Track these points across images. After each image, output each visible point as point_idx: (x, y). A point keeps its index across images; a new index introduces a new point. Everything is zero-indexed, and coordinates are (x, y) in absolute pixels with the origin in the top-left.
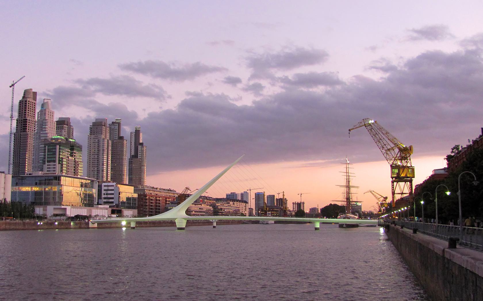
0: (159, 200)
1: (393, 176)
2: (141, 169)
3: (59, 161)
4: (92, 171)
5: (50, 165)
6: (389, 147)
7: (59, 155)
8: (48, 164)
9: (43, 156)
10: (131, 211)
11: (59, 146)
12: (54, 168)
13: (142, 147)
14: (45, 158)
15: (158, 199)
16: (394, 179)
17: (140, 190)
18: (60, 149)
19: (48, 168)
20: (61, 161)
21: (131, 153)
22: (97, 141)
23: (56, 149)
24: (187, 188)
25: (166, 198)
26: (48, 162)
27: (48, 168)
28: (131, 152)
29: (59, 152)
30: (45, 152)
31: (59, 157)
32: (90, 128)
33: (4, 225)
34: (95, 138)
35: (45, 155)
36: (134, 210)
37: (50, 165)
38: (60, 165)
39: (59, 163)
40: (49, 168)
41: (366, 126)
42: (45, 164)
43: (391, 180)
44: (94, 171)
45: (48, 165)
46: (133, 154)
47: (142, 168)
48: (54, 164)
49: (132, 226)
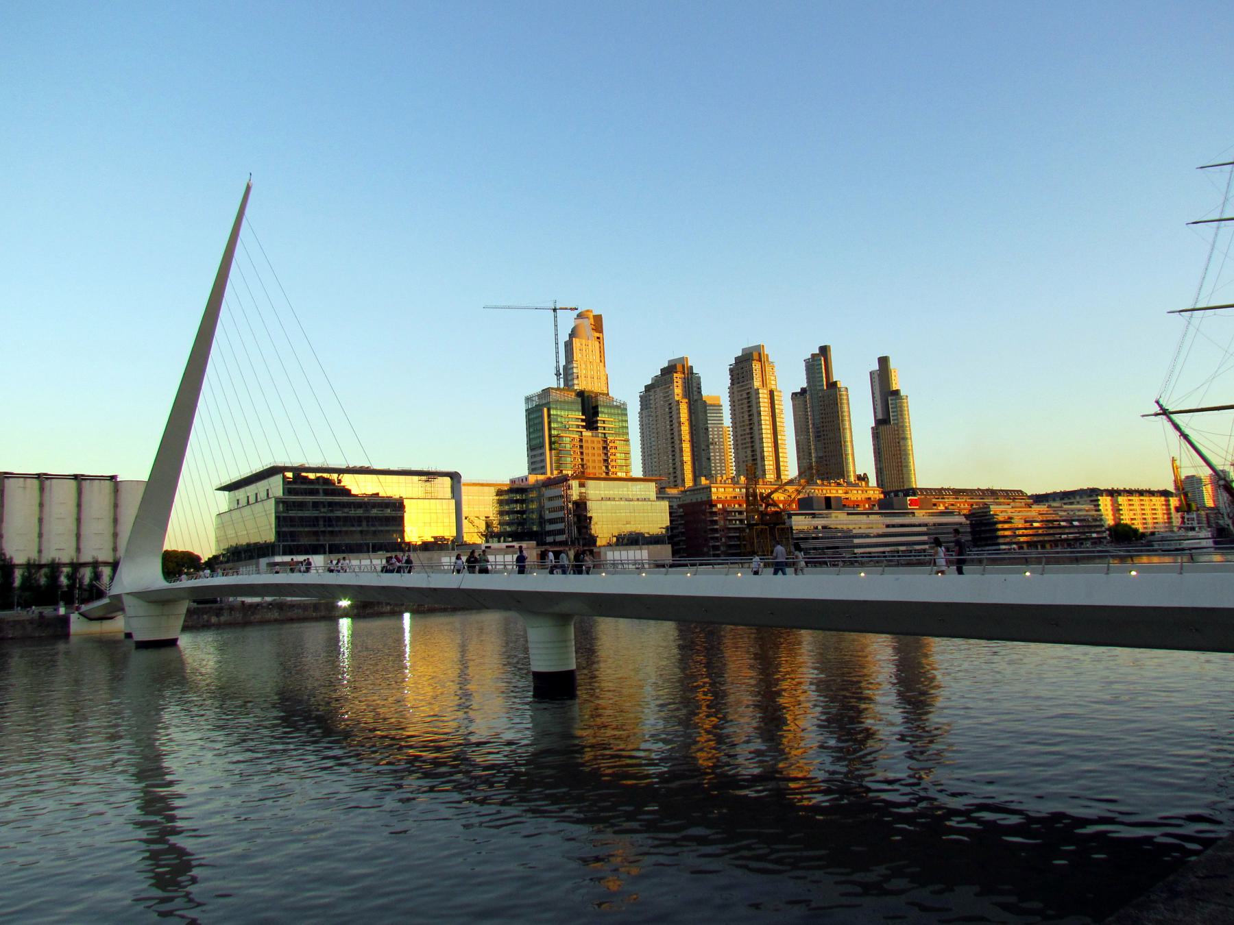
2: (899, 446)
3: (551, 443)
4: (744, 462)
7: (550, 429)
10: (641, 549)
13: (895, 400)
17: (703, 489)
18: (549, 415)
20: (554, 443)
21: (875, 416)
22: (745, 396)
28: (875, 413)
29: (549, 423)
31: (550, 436)
32: (730, 369)
34: (741, 391)
36: (651, 547)
39: (551, 449)
44: (747, 461)
46: (880, 417)
47: (901, 443)
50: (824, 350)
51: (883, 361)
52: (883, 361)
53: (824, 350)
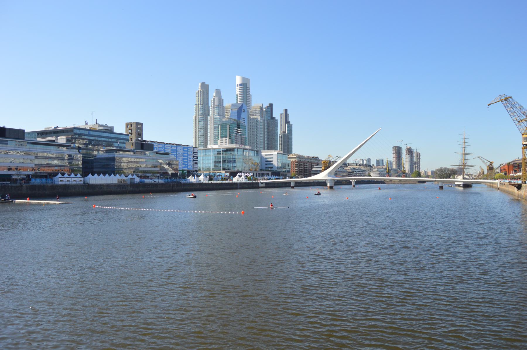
0: (307, 165)
1: (525, 143)
3: (229, 136)
5: (222, 140)
6: (522, 119)
8: (222, 139)
9: (217, 133)
11: (229, 125)
12: (226, 142)
14: (219, 135)
15: (306, 164)
16: (525, 146)
18: (229, 127)
19: (221, 142)
23: (227, 127)
24: (329, 156)
25: (312, 164)
26: (222, 137)
27: (221, 142)
30: (219, 130)
33: (199, 186)
35: (219, 133)
37: (222, 140)
38: (230, 140)
40: (222, 142)
41: (502, 101)
42: (219, 139)
43: (522, 146)
45: (221, 140)
47: (290, 140)
48: (226, 139)
49: (292, 185)
50: (271, 105)
51: (286, 111)
52: (286, 111)
53: (271, 105)
